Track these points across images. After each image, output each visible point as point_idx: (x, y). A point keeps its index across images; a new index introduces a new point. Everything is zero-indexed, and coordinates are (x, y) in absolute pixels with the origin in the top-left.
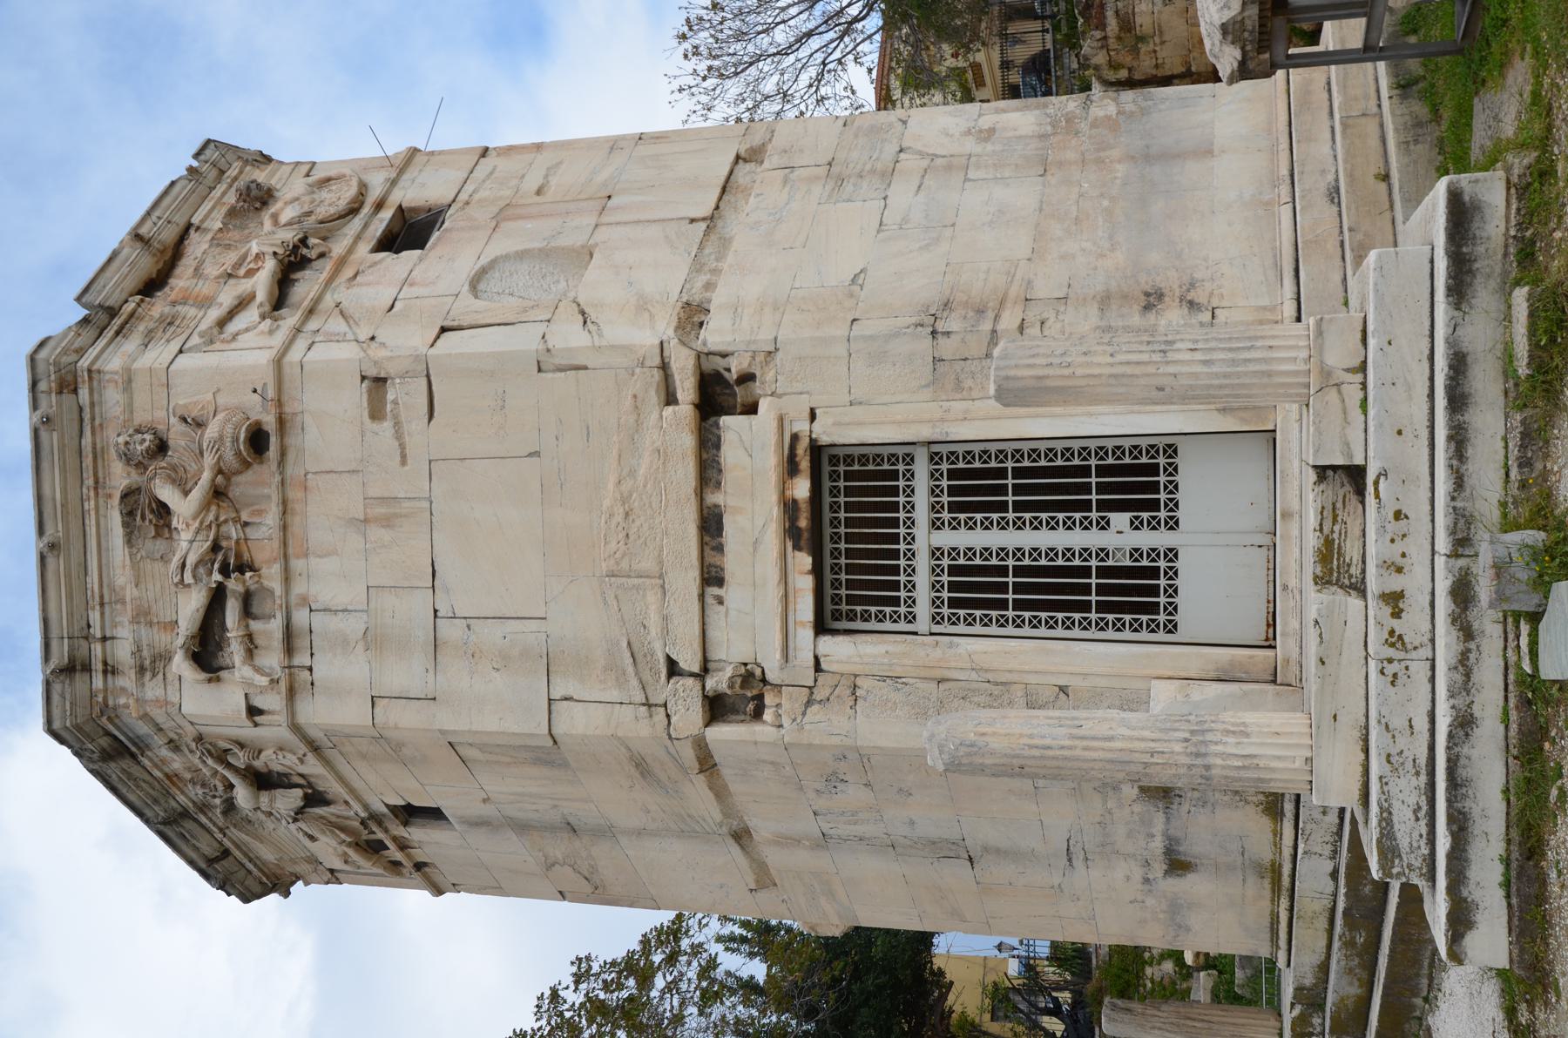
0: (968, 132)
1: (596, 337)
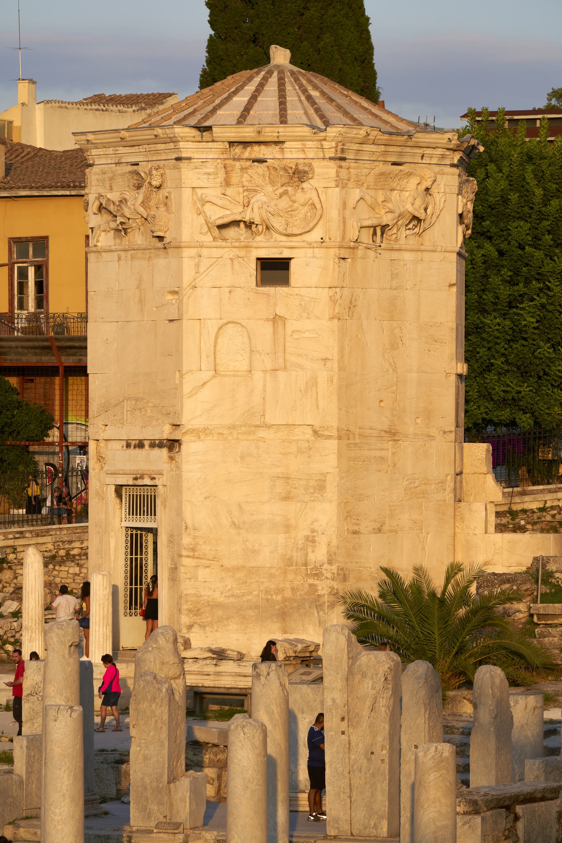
0: (313, 531)
1: (189, 395)
